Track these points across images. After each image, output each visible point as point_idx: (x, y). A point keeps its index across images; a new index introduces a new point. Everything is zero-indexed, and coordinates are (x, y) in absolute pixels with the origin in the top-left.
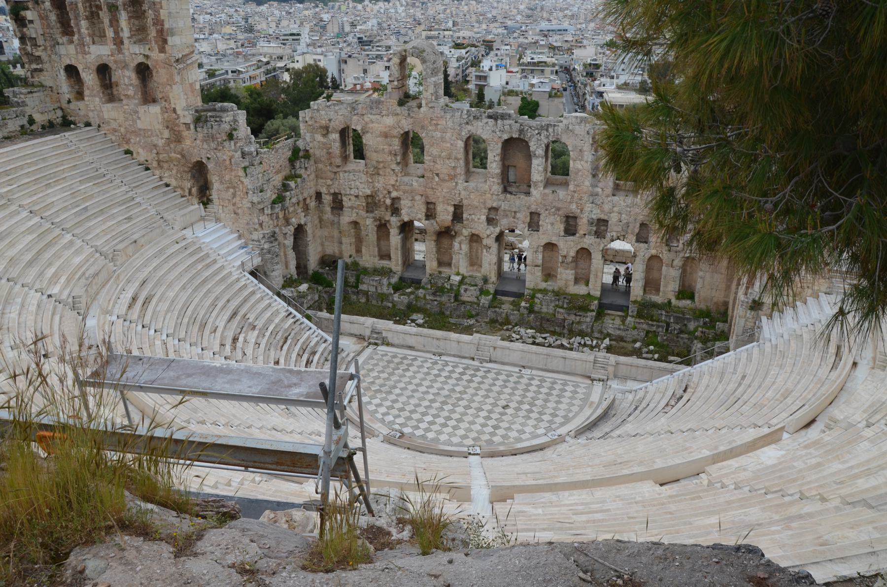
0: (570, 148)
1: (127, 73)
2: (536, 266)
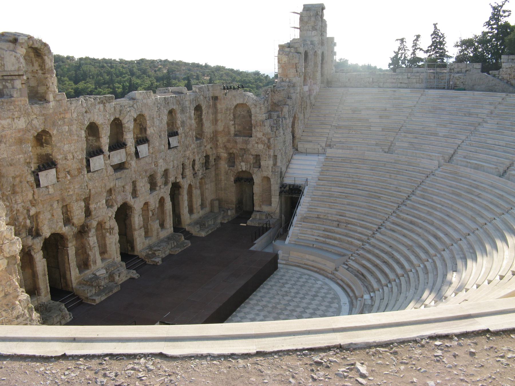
0: (147, 118)
2: (141, 228)
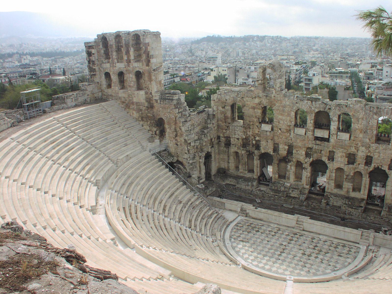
1: (131, 76)
